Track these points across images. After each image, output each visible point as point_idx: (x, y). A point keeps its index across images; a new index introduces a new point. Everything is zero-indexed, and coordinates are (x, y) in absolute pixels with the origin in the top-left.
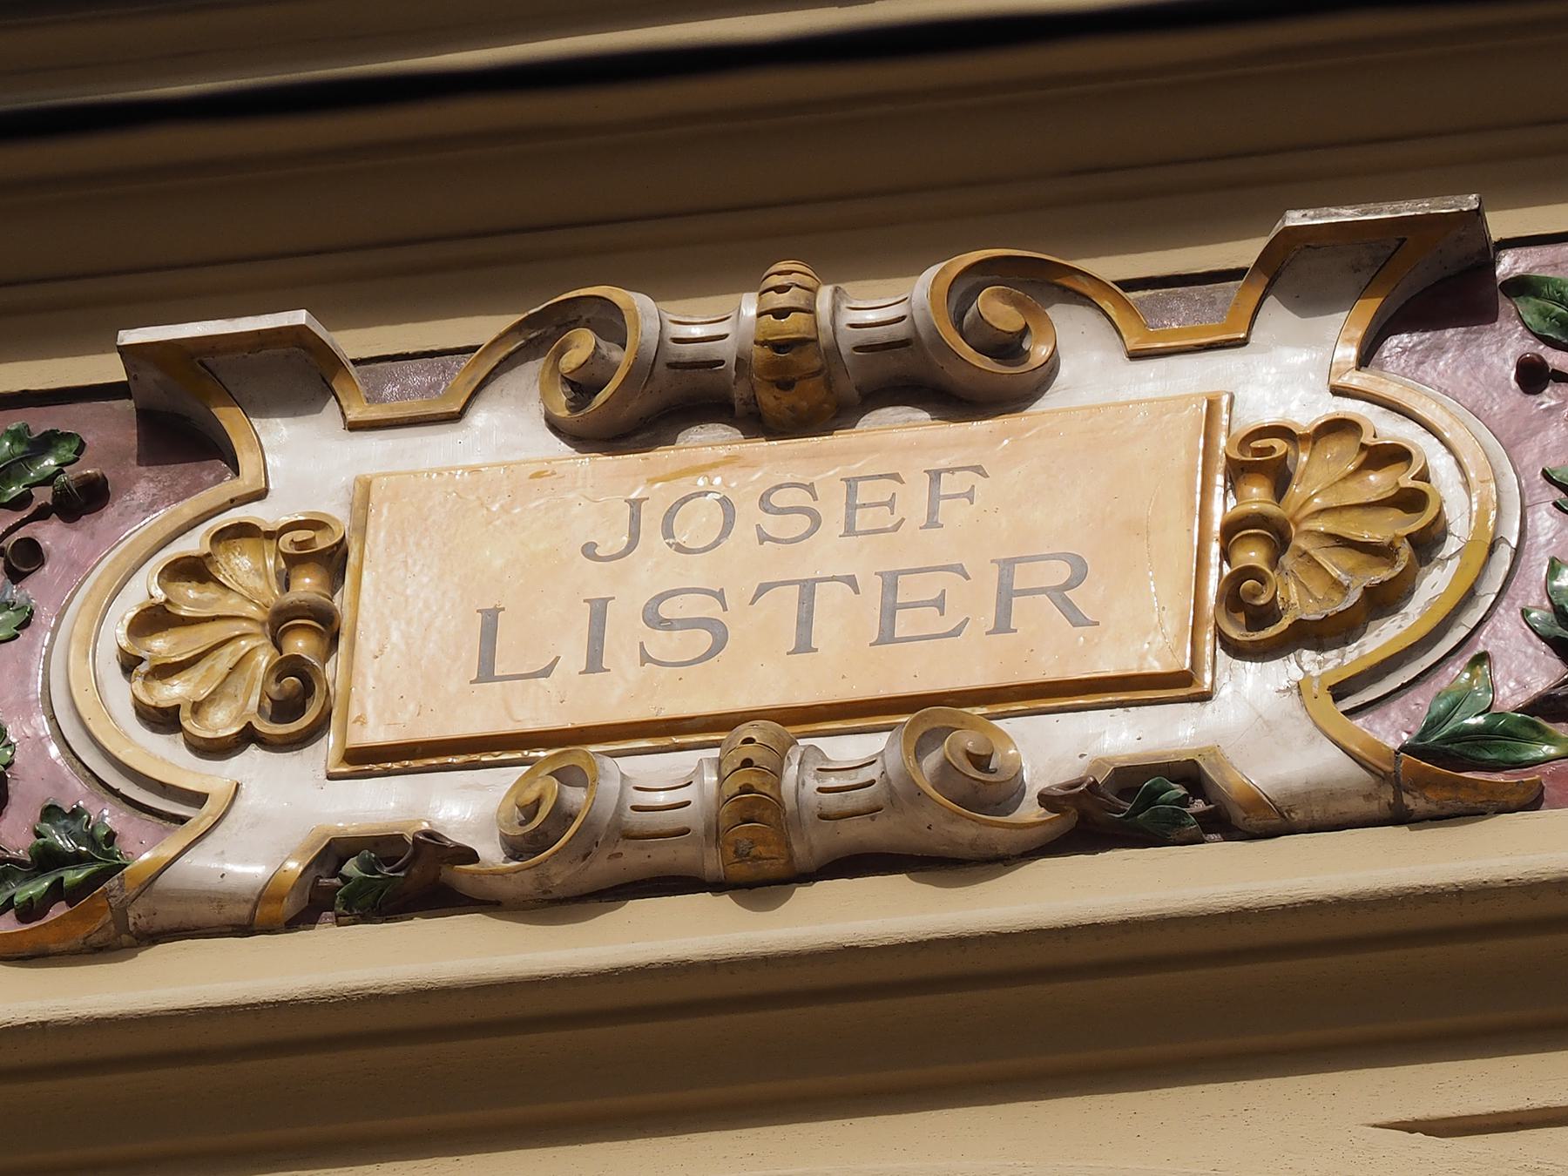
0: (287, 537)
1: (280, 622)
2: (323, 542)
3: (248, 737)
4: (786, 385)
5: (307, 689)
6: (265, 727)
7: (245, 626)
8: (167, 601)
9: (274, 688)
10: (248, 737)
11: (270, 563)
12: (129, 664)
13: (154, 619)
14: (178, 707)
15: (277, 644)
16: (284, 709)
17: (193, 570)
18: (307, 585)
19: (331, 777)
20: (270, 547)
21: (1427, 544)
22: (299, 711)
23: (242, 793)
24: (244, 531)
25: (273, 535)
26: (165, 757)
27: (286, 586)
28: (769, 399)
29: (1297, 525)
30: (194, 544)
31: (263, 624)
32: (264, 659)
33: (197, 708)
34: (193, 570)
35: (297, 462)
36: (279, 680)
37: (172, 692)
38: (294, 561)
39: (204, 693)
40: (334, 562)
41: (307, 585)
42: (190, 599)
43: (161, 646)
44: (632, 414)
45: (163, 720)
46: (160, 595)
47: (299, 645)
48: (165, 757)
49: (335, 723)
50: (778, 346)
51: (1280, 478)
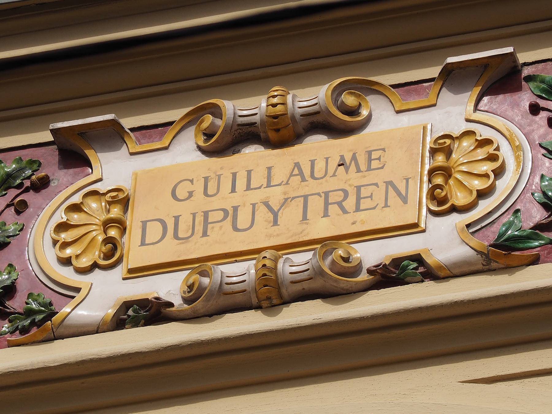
0: (109, 195)
1: (107, 224)
2: (121, 196)
3: (95, 266)
4: (277, 130)
5: (115, 248)
6: (102, 262)
7: (94, 227)
8: (67, 220)
9: (104, 249)
10: (95, 266)
11: (103, 204)
12: (55, 242)
13: (63, 227)
14: (71, 257)
15: (105, 232)
16: (107, 256)
17: (76, 208)
18: (116, 212)
19: (124, 279)
20: (103, 198)
21: (499, 172)
22: (112, 256)
23: (93, 285)
24: (95, 193)
25: (104, 194)
26: (67, 275)
27: (109, 211)
28: (272, 135)
29: (454, 169)
30: (77, 199)
31: (100, 226)
32: (100, 238)
33: (77, 256)
34: (76, 208)
35: (113, 168)
36: (105, 245)
37: (69, 252)
38: (110, 203)
39: (79, 252)
40: (125, 203)
41: (116, 212)
42: (75, 218)
43: (64, 236)
44: (227, 142)
45: (66, 262)
46: (65, 220)
47: (113, 233)
48: (67, 275)
49: (125, 259)
50: (275, 117)
51: (448, 152)
